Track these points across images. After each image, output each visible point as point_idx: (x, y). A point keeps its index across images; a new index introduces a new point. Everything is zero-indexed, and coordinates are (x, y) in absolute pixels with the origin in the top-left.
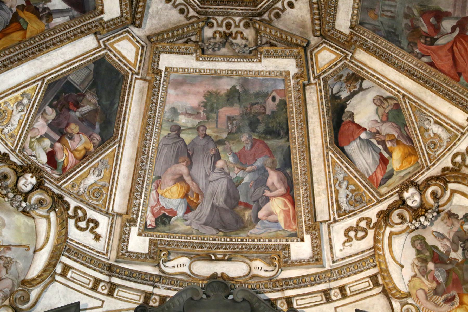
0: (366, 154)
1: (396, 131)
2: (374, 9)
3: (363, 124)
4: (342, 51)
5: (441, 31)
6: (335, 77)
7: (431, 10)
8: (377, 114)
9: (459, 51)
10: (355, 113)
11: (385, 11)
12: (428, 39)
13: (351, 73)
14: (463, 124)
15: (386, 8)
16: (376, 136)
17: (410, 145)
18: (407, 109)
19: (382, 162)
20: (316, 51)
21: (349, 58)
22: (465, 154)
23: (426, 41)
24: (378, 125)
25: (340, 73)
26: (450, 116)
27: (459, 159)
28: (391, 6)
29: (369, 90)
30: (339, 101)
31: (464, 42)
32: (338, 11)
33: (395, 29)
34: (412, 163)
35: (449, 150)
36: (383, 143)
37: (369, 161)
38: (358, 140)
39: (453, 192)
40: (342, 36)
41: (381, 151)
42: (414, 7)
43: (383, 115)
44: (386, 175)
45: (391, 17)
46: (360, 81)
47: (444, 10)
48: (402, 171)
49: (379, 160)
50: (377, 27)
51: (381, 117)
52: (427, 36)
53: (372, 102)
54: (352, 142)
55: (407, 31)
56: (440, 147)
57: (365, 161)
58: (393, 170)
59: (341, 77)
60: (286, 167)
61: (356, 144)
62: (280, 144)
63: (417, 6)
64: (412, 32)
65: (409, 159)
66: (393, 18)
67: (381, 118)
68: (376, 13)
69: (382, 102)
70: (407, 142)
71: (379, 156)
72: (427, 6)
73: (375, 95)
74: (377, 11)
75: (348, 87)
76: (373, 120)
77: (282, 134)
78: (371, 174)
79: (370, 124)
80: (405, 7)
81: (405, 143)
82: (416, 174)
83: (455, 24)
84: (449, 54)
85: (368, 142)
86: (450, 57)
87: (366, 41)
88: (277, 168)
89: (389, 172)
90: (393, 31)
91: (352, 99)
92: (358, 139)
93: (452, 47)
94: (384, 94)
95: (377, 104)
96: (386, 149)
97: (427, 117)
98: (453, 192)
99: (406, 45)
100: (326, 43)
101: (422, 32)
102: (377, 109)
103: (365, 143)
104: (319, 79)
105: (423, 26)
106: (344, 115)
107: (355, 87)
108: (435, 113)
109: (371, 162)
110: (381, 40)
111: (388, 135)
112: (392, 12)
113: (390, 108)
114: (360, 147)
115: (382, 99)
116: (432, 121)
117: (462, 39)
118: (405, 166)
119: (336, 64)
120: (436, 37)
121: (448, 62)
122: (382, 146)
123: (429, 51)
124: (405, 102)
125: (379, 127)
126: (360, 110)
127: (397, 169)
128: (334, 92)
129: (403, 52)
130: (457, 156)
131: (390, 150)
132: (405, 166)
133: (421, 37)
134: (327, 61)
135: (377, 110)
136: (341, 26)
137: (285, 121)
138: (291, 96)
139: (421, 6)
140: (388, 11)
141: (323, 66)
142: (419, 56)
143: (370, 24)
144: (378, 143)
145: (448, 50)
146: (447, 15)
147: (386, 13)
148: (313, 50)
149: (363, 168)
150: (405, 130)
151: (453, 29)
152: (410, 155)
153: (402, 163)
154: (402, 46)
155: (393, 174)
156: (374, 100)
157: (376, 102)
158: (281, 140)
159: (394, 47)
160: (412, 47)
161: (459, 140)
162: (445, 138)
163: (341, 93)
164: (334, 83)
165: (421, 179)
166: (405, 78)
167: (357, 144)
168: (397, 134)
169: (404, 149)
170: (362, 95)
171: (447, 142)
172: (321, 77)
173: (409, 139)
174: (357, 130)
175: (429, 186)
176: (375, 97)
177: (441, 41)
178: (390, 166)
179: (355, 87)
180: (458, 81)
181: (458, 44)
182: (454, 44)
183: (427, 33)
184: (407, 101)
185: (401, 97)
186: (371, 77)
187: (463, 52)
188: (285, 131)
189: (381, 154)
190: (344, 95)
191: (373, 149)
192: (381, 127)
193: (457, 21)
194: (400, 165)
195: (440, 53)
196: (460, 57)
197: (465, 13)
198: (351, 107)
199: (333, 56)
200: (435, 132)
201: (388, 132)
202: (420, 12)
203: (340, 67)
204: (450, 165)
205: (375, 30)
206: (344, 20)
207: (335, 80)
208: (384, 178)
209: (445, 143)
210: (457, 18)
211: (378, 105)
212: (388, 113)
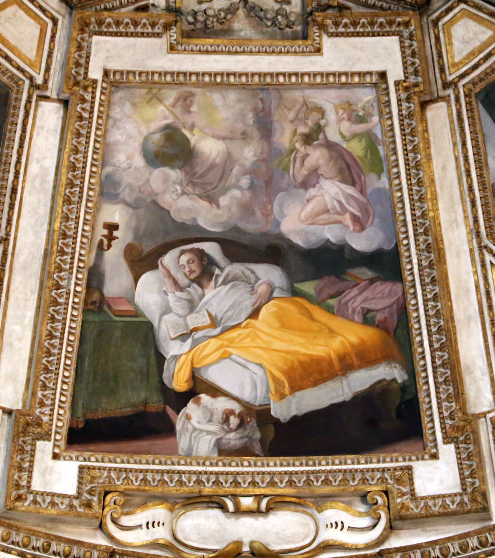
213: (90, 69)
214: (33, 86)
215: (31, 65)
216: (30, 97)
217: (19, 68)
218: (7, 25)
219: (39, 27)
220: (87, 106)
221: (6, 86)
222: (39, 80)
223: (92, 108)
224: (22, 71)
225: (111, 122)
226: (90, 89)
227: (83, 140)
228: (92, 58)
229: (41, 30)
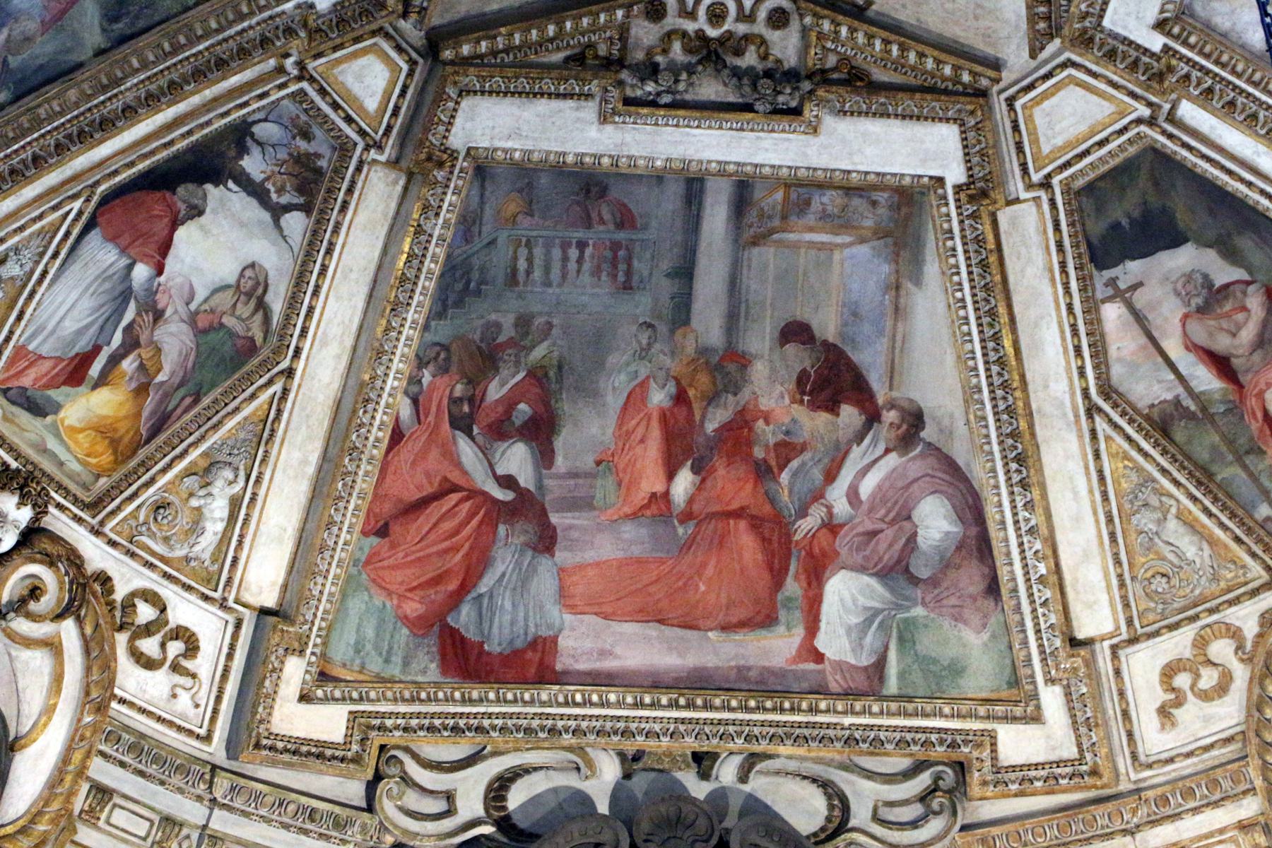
0: (87, 303)
1: (172, 374)
2: (530, 214)
3: (176, 257)
4: (389, 128)
5: (495, 445)
6: (304, 117)
7: (553, 402)
8: (216, 291)
9: (449, 511)
10: (203, 219)
11: (530, 253)
12: (466, 408)
13: (323, 163)
14: (247, 589)
15: (538, 252)
16: (147, 312)
17: (144, 433)
18: (253, 396)
19: (77, 361)
20: (386, 46)
21: (373, 154)
22: (167, 628)
23: (461, 399)
24: (182, 309)
25: (317, 131)
26: (261, 539)
27: (145, 612)
28: (547, 269)
29: (280, 240)
30: (232, 153)
31: (475, 522)
32: (517, 100)
33: (478, 293)
34: (93, 461)
35: (166, 576)
36: (131, 344)
37: (67, 323)
38: (124, 262)
39: (53, 646)
40: (441, 128)
41: (105, 348)
42: (554, 344)
43: (212, 311)
44: (37, 395)
45: (514, 271)
46: (301, 200)
47: (559, 443)
48: (62, 441)
49: (77, 355)
50: (475, 229)
51: (206, 307)
52: (475, 401)
53: (245, 264)
54: (117, 245)
55: (478, 332)
56: (166, 539)
57: (69, 310)
58: (57, 408)
59: (307, 135)
60: (14, 83)
61: (113, 259)
62: (87, 35)
63: (556, 354)
64: (479, 348)
65: (99, 448)
66: (512, 278)
67: (203, 308)
68: (520, 217)
69: (249, 295)
70: (149, 419)
71: (90, 347)
72: (561, 388)
73: (267, 265)
74: (525, 221)
75: (277, 169)
76: (191, 285)
77: (116, 26)
78: (31, 347)
79: (179, 280)
80: (549, 314)
81: (145, 413)
82: (67, 493)
83: (522, 483)
84: (436, 485)
85: (125, 295)
86: (429, 490)
87: (437, 215)
88: (10, 58)
89: (49, 399)
90: (472, 285)
91: (243, 195)
92: (128, 261)
93: (455, 488)
94: (276, 294)
95: (243, 281)
96: (115, 360)
97: (242, 467)
98: (53, 646)
99: (437, 339)
100: (410, 74)
101: (482, 386)
102: (228, 287)
103: (120, 288)
104: (300, 78)
105: (502, 385)
106: (191, 186)
107: (280, 191)
108: (262, 492)
109: (66, 333)
110: (441, 252)
111: (159, 350)
112: (528, 273)
113: (239, 328)
114: (104, 277)
115: (260, 291)
116: (237, 488)
117: (482, 512)
118: (76, 442)
119: (349, 120)
120: (476, 430)
121: (412, 486)
122: (123, 345)
123: (431, 418)
124: (270, 382)
125: (176, 312)
126: (215, 231)
127: (62, 421)
128: (256, 129)
129: (416, 335)
130: (154, 605)
131: (116, 372)
132: (76, 442)
133: (470, 382)
134: (356, 88)
135: (225, 288)
136: (472, 120)
137: (157, 18)
138: (241, 17)
139: (560, 367)
140: (530, 260)
141: (340, 78)
142: (415, 389)
143: (482, 202)
144: (129, 328)
145: (445, 479)
146: (545, 456)
147: (523, 252)
148: (387, 36)
149: (44, 317)
150: (183, 399)
151: (508, 482)
152: (114, 443)
153: (81, 430)
154: (433, 323)
155: (45, 415)
156: (252, 265)
157: (248, 273)
158: (97, 30)
159: (427, 303)
160: (436, 358)
161: (206, 598)
162: (197, 548)
163: (256, 151)
164: (285, 121)
165: (58, 522)
166: (339, 357)
167: (111, 265)
168: (165, 378)
169: (126, 417)
170: (260, 222)
171: (187, 559)
172: (305, 85)
173: (161, 422)
174: (154, 246)
175: (51, 562)
176: (260, 266)
177: (467, 451)
178: (67, 395)
179: (280, 191)
180: (365, 533)
181: (467, 505)
182: (465, 493)
183: (482, 400)
184: (277, 387)
185: (284, 365)
186: (325, 243)
187: (448, 526)
188: (129, 32)
189: (96, 350)
190: (253, 164)
191: (108, 319)
192: (176, 317)
193: (532, 488)
194: (78, 425)
195: (434, 454)
196: (433, 520)
197: (557, 512)
198: (221, 200)
199: (372, 104)
200: (205, 511)
201: (166, 348)
202: (542, 367)
203: (340, 130)
204: (119, 595)
205: (468, 224)
206: (490, 124)
207: (294, 120)
208: (29, 393)
209: (179, 553)
210: (540, 486)
211: (238, 286)
212: (222, 325)
213: (1147, 45)
214: (1151, 122)
215: (1122, 115)
216: (1164, 132)
217: (1121, 132)
218: (1057, 128)
219: (1072, 86)
220: (1195, 74)
221: (1145, 150)
222: (1145, 112)
223: (1202, 68)
224: (1125, 129)
225: (1234, 37)
226: (1174, 62)
227: (1241, 100)
228: (1132, 37)
229: (1078, 85)
